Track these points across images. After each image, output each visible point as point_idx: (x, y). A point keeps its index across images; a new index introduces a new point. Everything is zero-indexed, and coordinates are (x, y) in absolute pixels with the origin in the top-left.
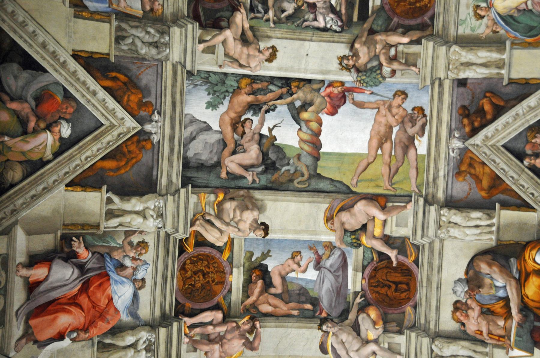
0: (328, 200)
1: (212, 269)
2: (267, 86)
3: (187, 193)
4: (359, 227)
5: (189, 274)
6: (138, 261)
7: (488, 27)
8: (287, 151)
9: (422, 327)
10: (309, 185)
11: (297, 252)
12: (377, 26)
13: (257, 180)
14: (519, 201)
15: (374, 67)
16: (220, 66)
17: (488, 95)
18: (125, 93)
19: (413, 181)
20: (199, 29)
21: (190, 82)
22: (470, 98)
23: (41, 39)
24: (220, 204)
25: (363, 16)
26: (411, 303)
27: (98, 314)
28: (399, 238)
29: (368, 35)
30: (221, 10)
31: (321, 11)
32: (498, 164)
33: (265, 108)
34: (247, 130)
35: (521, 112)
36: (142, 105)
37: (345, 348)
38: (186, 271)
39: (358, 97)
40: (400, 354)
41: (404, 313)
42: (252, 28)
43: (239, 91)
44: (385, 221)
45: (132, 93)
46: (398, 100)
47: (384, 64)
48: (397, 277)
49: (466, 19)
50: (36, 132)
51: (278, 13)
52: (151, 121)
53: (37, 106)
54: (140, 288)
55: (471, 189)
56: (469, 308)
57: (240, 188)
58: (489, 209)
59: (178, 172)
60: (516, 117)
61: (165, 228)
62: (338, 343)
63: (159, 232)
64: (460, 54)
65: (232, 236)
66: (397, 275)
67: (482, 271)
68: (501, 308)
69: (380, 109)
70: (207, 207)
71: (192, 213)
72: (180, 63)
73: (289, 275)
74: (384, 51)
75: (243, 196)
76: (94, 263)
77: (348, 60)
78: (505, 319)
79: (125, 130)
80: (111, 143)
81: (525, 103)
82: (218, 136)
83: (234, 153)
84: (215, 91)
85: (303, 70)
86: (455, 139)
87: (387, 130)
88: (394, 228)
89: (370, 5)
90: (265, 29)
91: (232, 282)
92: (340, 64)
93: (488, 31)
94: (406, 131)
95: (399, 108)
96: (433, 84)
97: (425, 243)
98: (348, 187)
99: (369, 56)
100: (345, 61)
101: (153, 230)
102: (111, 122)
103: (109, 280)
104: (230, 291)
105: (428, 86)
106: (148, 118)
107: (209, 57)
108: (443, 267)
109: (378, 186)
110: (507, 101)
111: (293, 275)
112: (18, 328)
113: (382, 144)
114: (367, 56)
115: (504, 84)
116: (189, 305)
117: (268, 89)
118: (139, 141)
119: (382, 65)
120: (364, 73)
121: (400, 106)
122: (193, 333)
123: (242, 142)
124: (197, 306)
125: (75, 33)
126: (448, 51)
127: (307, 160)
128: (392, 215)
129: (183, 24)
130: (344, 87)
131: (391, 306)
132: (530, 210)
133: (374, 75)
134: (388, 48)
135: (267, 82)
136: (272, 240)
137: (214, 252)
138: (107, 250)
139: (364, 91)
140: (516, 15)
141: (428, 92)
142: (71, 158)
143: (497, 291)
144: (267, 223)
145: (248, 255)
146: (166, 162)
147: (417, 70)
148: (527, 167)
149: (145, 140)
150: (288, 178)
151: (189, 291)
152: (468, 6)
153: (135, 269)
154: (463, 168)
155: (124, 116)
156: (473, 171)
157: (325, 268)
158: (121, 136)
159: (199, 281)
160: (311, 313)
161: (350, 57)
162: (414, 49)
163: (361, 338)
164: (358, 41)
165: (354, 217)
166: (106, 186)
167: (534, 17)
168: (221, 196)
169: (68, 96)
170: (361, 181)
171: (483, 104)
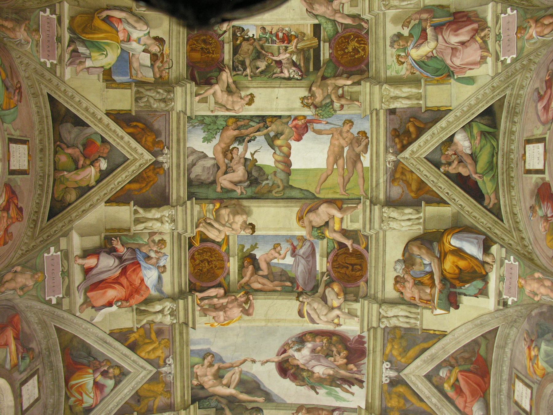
1: (214, 258)
3: (192, 204)
4: (323, 224)
5: (198, 262)
7: (407, 70)
8: (265, 169)
9: (373, 297)
13: (244, 192)
14: (438, 199)
15: (328, 103)
16: (212, 111)
17: (412, 120)
19: (361, 187)
22: (399, 122)
23: (84, 106)
24: (217, 211)
25: (317, 67)
26: (364, 279)
27: (134, 290)
29: (322, 80)
31: (286, 65)
33: (247, 139)
34: (234, 156)
35: (436, 132)
36: (155, 143)
37: (317, 313)
38: (195, 260)
39: (317, 126)
40: (356, 316)
41: (359, 286)
42: (234, 82)
44: (342, 219)
45: (148, 135)
46: (347, 127)
47: (335, 101)
48: (353, 260)
50: (84, 167)
51: (254, 70)
53: (84, 149)
54: (163, 272)
55: (403, 191)
56: (405, 281)
57: (232, 199)
58: (417, 206)
59: (184, 189)
62: (311, 310)
66: (353, 258)
67: (414, 253)
68: (428, 280)
70: (208, 213)
71: (197, 218)
74: (333, 91)
75: (234, 204)
76: (128, 255)
77: (308, 99)
78: (431, 288)
79: (144, 162)
81: (438, 125)
82: (212, 162)
83: (226, 173)
88: (349, 224)
89: (322, 59)
90: (244, 82)
92: (302, 103)
93: (408, 73)
94: (354, 150)
96: (371, 113)
100: (306, 101)
101: (168, 231)
103: (140, 266)
104: (228, 274)
105: (368, 115)
107: (203, 105)
109: (335, 192)
110: (426, 124)
111: (275, 261)
112: (80, 298)
113: (337, 160)
115: (423, 111)
118: (154, 169)
121: (348, 131)
122: (203, 303)
123: (232, 164)
124: (205, 285)
125: (107, 99)
126: (381, 88)
127: (282, 175)
132: (446, 205)
133: (328, 109)
137: (215, 246)
138: (137, 246)
142: (108, 183)
143: (425, 268)
145: (241, 247)
146: (175, 183)
147: (359, 104)
148: (443, 173)
149: (159, 168)
150: (268, 190)
151: (198, 274)
152: (392, 57)
153: (158, 259)
154: (398, 175)
155: (143, 152)
156: (404, 178)
160: (290, 289)
162: (356, 88)
163: (328, 306)
164: (314, 85)
167: (438, 62)
168: (218, 205)
169: (104, 140)
170: (323, 189)
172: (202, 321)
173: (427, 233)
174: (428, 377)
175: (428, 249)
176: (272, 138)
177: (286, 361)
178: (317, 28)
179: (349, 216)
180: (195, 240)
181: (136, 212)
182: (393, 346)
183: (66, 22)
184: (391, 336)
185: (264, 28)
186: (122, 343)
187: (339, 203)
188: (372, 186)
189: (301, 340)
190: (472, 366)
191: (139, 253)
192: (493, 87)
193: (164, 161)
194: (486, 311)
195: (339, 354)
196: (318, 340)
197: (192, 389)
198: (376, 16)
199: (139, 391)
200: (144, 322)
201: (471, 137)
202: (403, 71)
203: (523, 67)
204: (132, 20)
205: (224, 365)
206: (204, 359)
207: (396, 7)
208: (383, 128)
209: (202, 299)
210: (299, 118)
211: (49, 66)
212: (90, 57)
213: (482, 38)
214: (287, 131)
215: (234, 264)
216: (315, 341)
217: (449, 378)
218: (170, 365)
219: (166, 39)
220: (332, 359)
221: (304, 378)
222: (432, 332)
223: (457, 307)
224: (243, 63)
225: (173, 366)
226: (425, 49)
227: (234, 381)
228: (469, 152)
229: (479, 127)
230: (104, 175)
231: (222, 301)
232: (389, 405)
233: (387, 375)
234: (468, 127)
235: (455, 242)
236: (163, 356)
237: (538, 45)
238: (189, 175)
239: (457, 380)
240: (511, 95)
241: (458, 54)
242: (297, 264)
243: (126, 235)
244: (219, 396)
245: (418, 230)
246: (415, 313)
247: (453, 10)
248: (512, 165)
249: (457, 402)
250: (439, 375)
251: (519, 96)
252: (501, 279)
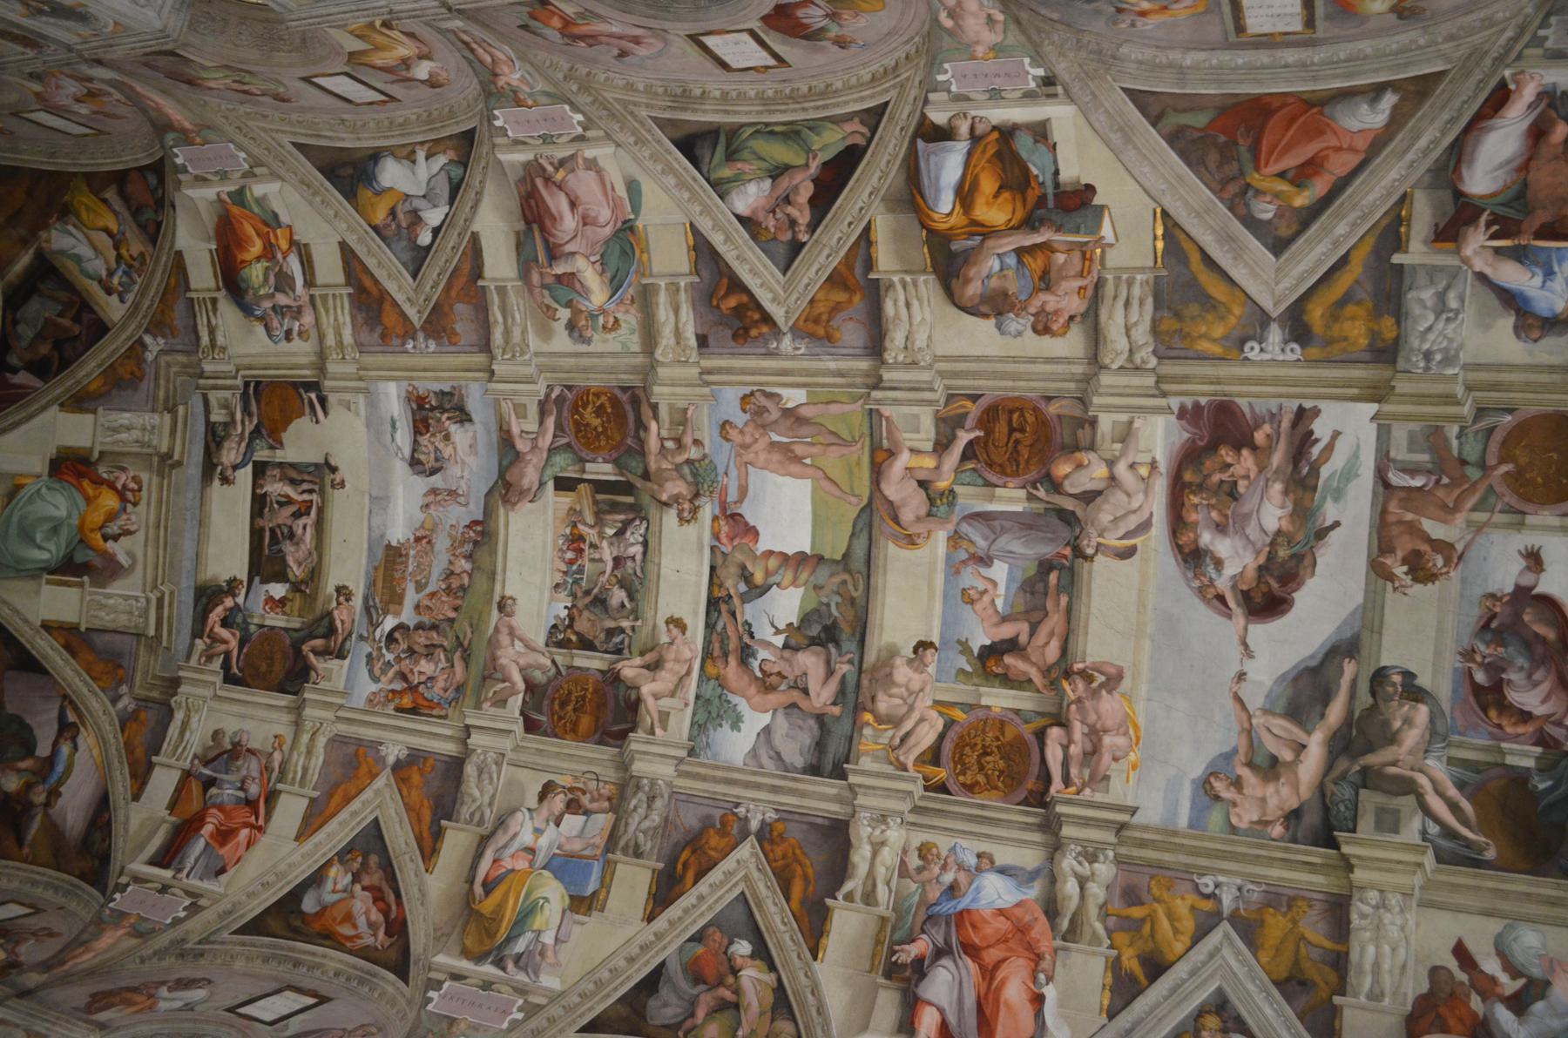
0: (882, 542)
3: (856, 772)
5: (981, 779)
7: (627, 312)
9: (1084, 385)
13: (849, 656)
14: (863, 244)
16: (686, 705)
19: (847, 408)
23: (622, 963)
24: (880, 720)
25: (626, 488)
26: (1042, 405)
27: (1019, 935)
28: (937, 426)
30: (616, 697)
33: (747, 639)
34: (775, 670)
35: (734, 253)
36: (723, 832)
37: (1125, 516)
38: (977, 783)
39: (732, 495)
40: (1131, 423)
41: (1059, 416)
42: (642, 654)
44: (912, 450)
46: (733, 434)
48: (1001, 428)
50: (737, 991)
51: (625, 613)
52: (746, 820)
53: (705, 983)
54: (992, 862)
56: (1042, 311)
57: (858, 685)
59: (823, 784)
65: (930, 703)
73: (1000, 608)
81: (722, 249)
82: (780, 716)
83: (806, 691)
88: (922, 435)
89: (613, 478)
93: (633, 310)
94: (776, 422)
98: (862, 510)
100: (686, 514)
101: (903, 832)
103: (968, 911)
104: (1017, 712)
107: (672, 721)
109: (858, 464)
110: (721, 274)
111: (999, 603)
116: (1031, 783)
118: (772, 841)
121: (741, 432)
123: (791, 678)
126: (663, 365)
127: (822, 574)
131: (1048, 440)
136: (942, 637)
137: (952, 735)
138: (924, 909)
140: (609, 275)
142: (780, 947)
143: (1009, 267)
145: (961, 677)
151: (1008, 781)
152: (605, 341)
153: (961, 867)
154: (821, 332)
156: (825, 317)
162: (664, 412)
169: (698, 938)
170: (852, 488)
172: (1120, 789)
173: (933, 266)
174: (1279, 247)
175: (966, 261)
177: (1246, 597)
178: (563, 485)
179: (906, 435)
181: (849, 897)
182: (1201, 337)
183: (465, 965)
184: (1176, 341)
185: (557, 586)
186: (1140, 992)
187: (881, 456)
188: (842, 386)
189: (1193, 557)
190: (1241, 142)
191: (938, 908)
192: (636, 143)
193: (760, 817)
194: (1081, 121)
195: (1230, 465)
196: (1193, 517)
197: (1294, 840)
198: (541, 369)
199: (1275, 976)
200: (1099, 926)
201: (738, 179)
202: (630, 319)
203: (584, 88)
204: (501, 839)
205: (1242, 751)
206: (1217, 798)
207: (524, 332)
209: (1067, 781)
211: (520, 1016)
212: (539, 933)
213: (557, 170)
214: (739, 557)
215: (996, 696)
216: (1196, 523)
217: (1277, 195)
218: (1217, 886)
219: (546, 777)
220: (1242, 486)
221: (1293, 556)
222: (1160, 245)
223: (1090, 189)
224: (610, 633)
225: (1221, 879)
226: (590, 276)
227: (1290, 732)
228: (768, 182)
229: (719, 165)
230: (762, 952)
231: (1077, 736)
232: (1364, 342)
233: (1277, 349)
234: (721, 188)
235: (945, 203)
236: (1191, 898)
237: (529, 67)
238: (795, 770)
239: (1282, 175)
240: (648, 106)
241: (592, 214)
242: (1008, 555)
243: (894, 929)
244: (1325, 775)
245: (928, 285)
246: (1117, 287)
247: (521, 226)
248: (787, 91)
249: (1341, 171)
250: (1270, 222)
251: (649, 91)
252: (996, 95)
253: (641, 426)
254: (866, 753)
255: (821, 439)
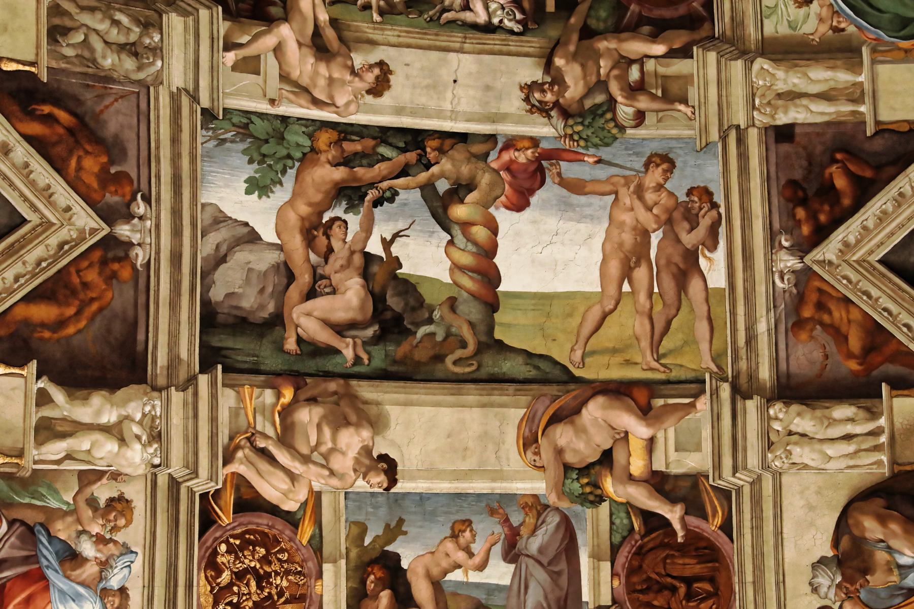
0: (524, 399)
1: (276, 567)
2: (374, 148)
3: (213, 384)
5: (225, 577)
6: (111, 545)
7: (821, 20)
8: (422, 290)
10: (478, 369)
11: (464, 522)
12: (598, 19)
13: (365, 357)
15: (599, 106)
16: (272, 102)
17: (839, 156)
18: (71, 152)
19: (704, 346)
20: (224, 19)
21: (210, 133)
22: (804, 163)
24: (287, 412)
32: (877, 300)
33: (371, 195)
34: (336, 244)
38: (219, 573)
39: (570, 170)
42: (334, 22)
43: (315, 156)
44: (651, 441)
45: (87, 153)
46: (655, 176)
47: (620, 99)
48: (691, 567)
49: (776, 6)
52: (129, 217)
55: (826, 357)
58: (868, 396)
59: (191, 335)
60: (899, 199)
61: (168, 466)
63: (155, 475)
64: (773, 75)
65: (316, 486)
66: (687, 561)
67: (868, 535)
69: (620, 196)
70: (259, 418)
71: (227, 432)
72: (185, 90)
73: (450, 577)
74: (615, 72)
75: (335, 393)
77: (543, 91)
80: (44, 264)
82: (274, 257)
83: (311, 294)
84: (264, 156)
85: (449, 114)
86: (783, 252)
87: (638, 239)
88: (673, 455)
90: (364, 26)
91: (322, 596)
92: (527, 100)
93: (824, 29)
94: (678, 241)
95: (659, 191)
97: (741, 483)
98: (565, 368)
99: (586, 83)
100: (537, 95)
101: (141, 471)
102: (43, 216)
103: (47, 588)
105: (716, 143)
106: (124, 210)
107: (248, 79)
108: (785, 536)
109: (628, 363)
111: (457, 576)
113: (631, 269)
114: (581, 83)
115: (868, 134)
117: (378, 154)
118: (104, 262)
119: (616, 101)
120: (580, 120)
121: (660, 187)
123: (328, 270)
126: (748, 69)
127: (472, 310)
128: (665, 425)
129: (190, 9)
130: (539, 150)
134: (625, 66)
135: (374, 138)
137: (280, 527)
138: (41, 518)
139: (581, 157)
141: (715, 155)
143: (903, 577)
144: (392, 456)
145: (355, 530)
147: (689, 111)
149: (119, 260)
150: (431, 353)
153: (105, 565)
154: (807, 313)
155: (71, 203)
156: (826, 318)
157: (528, 556)
158: (66, 247)
159: (249, 594)
161: (547, 86)
162: (680, 66)
164: (560, 51)
165: (584, 436)
166: (35, 362)
170: (593, 353)
171: (831, 174)
173: (901, 473)
176: (442, 198)
180: (222, 503)
181: (43, 398)
187: (641, 395)
208: (758, 180)
210: (520, 145)
214: (485, 180)
238: (206, 289)
242: (522, 583)
253: (658, 30)
254: (240, 399)
255: (658, 307)
